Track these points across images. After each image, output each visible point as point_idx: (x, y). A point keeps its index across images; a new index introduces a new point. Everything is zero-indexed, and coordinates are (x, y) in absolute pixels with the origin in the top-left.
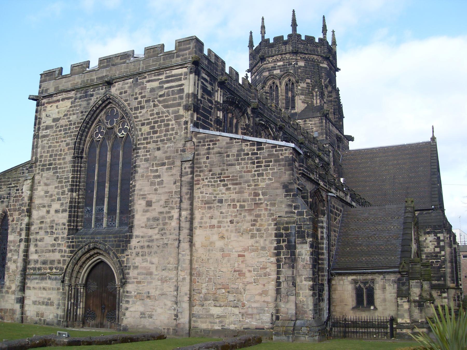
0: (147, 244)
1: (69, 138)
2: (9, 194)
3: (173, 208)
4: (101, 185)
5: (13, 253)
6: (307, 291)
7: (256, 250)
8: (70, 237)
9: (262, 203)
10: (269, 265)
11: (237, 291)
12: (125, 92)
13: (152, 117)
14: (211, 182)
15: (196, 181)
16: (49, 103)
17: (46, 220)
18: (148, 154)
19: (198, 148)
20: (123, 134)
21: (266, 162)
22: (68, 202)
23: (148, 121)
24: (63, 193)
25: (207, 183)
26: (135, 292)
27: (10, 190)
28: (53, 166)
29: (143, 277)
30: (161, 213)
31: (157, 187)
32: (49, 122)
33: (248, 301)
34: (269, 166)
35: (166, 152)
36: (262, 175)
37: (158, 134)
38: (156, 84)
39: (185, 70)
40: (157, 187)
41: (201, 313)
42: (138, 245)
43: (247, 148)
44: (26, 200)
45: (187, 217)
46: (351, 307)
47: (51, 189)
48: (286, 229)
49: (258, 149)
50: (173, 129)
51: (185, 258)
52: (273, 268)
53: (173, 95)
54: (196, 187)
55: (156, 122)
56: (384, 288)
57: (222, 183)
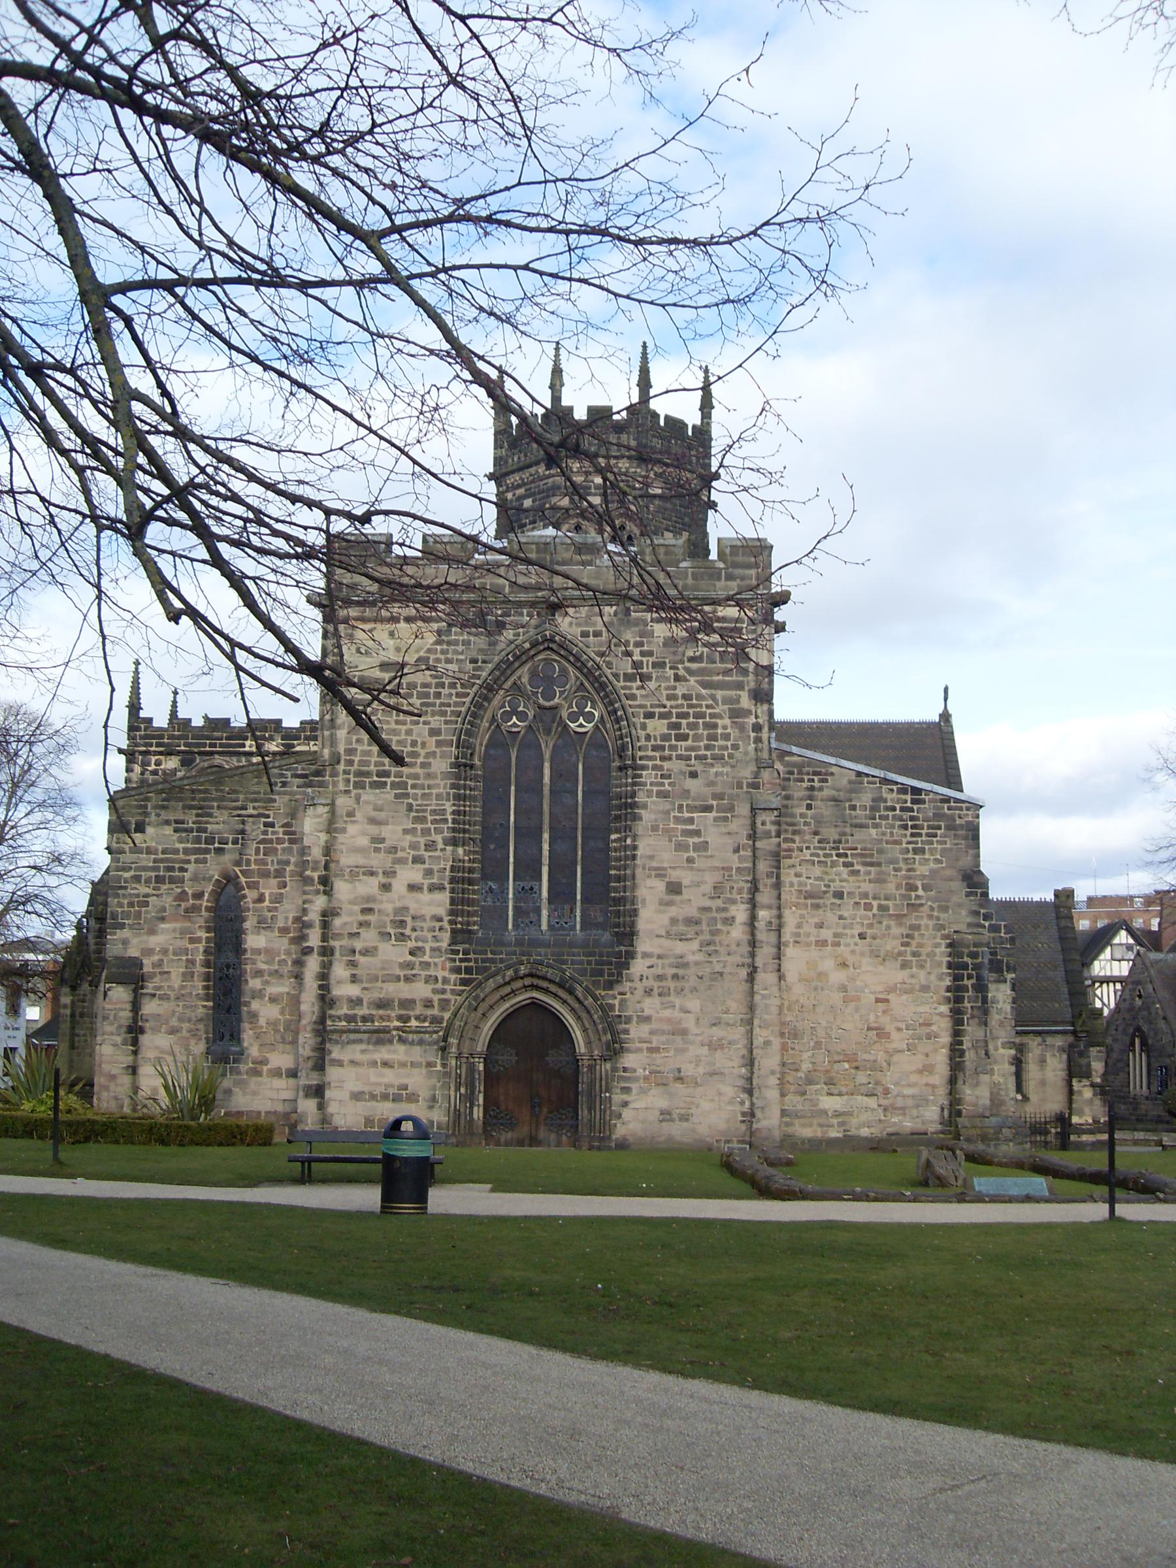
1: (437, 718)
2: (243, 832)
3: (733, 902)
4: (529, 834)
5: (266, 977)
6: (1007, 1066)
7: (910, 991)
8: (460, 948)
9: (922, 905)
10: (936, 1018)
11: (874, 1066)
13: (673, 703)
14: (818, 855)
15: (786, 850)
17: (382, 907)
18: (667, 781)
19: (786, 783)
20: (581, 726)
21: (929, 827)
22: (448, 868)
23: (662, 710)
24: (430, 846)
25: (808, 858)
26: (645, 1069)
27: (243, 823)
28: (392, 779)
29: (664, 1038)
30: (707, 909)
31: (692, 854)
33: (896, 1084)
34: (935, 836)
35: (712, 784)
36: (922, 851)
37: (689, 742)
40: (692, 854)
41: (800, 1107)
42: (646, 972)
43: (891, 797)
44: (316, 853)
45: (770, 922)
47: (392, 833)
48: (974, 955)
49: (914, 802)
50: (726, 737)
51: (768, 1002)
52: (942, 1027)
53: (722, 661)
54: (786, 862)
55: (685, 716)
56: (1042, 1061)
57: (842, 860)
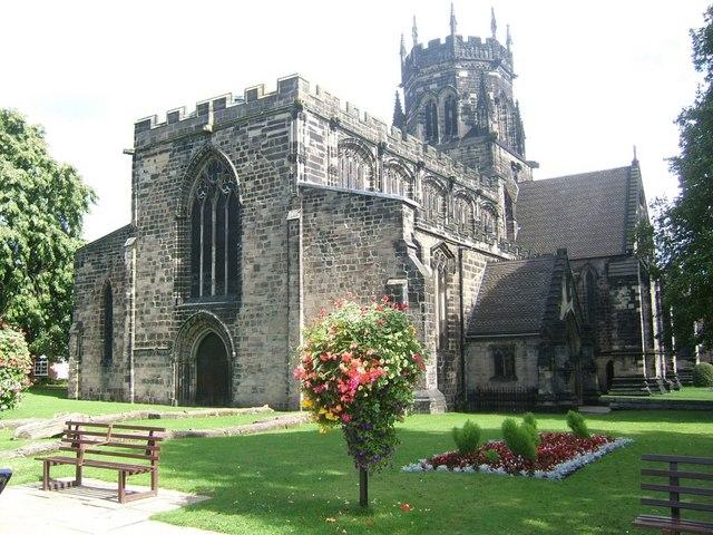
0: (255, 313)
12: (227, 142)
16: (146, 157)
32: (147, 179)
38: (257, 133)
39: (287, 115)
46: (488, 377)
49: (367, 204)
50: (278, 184)
